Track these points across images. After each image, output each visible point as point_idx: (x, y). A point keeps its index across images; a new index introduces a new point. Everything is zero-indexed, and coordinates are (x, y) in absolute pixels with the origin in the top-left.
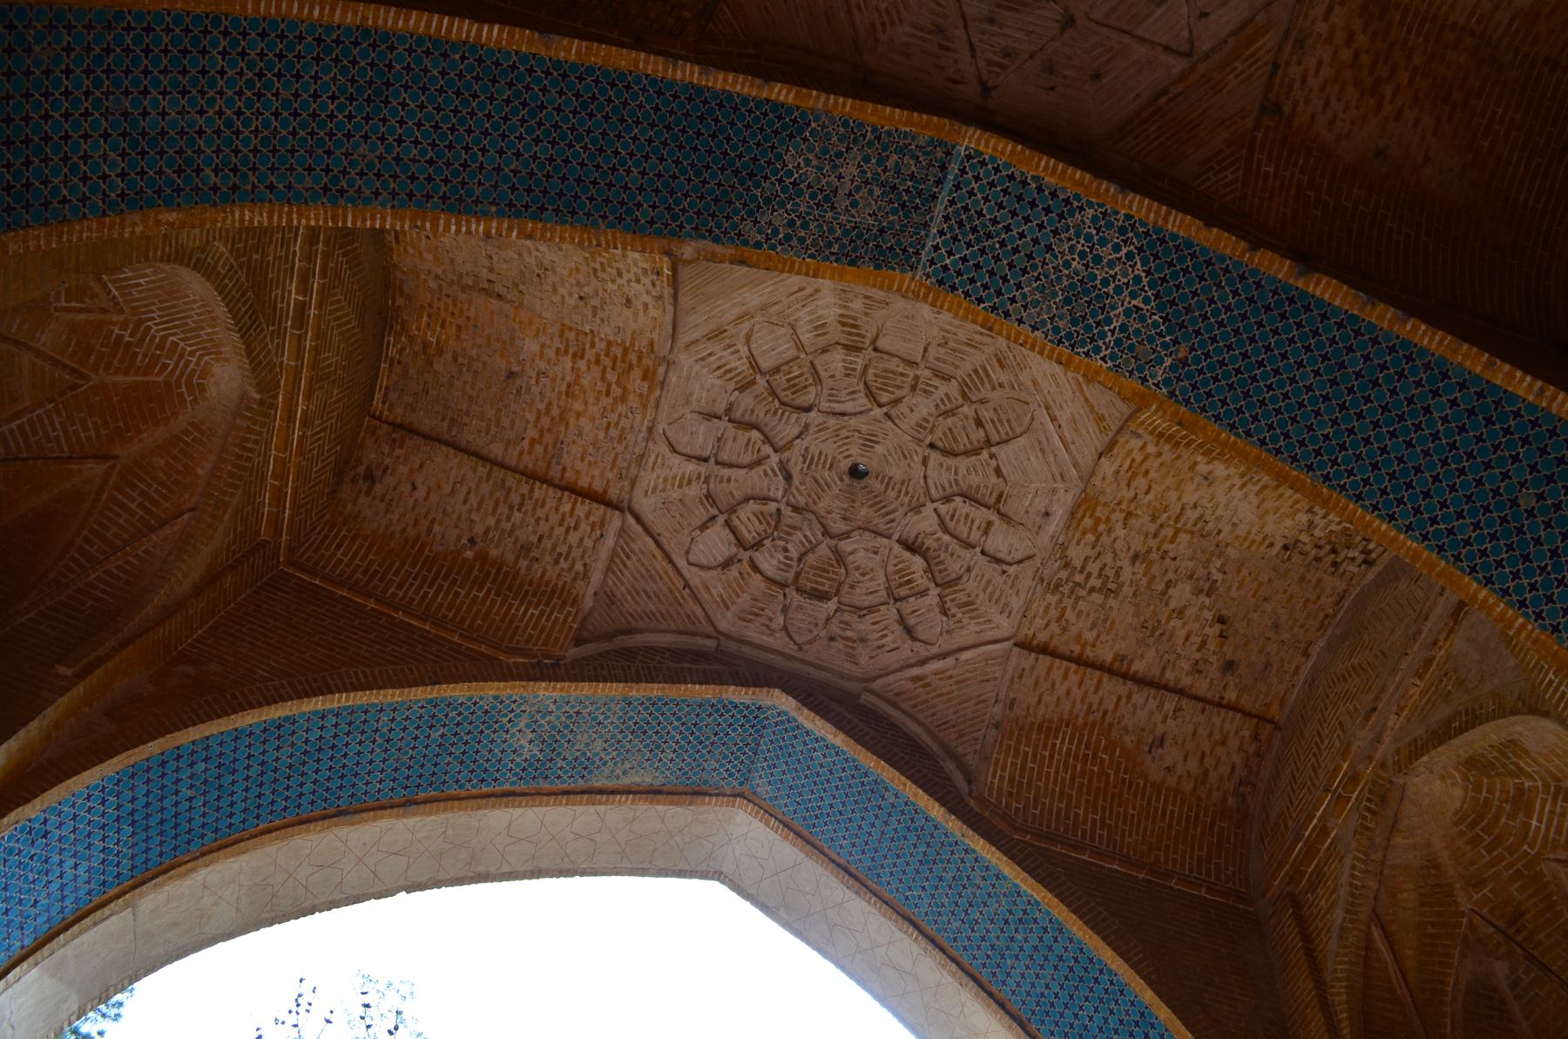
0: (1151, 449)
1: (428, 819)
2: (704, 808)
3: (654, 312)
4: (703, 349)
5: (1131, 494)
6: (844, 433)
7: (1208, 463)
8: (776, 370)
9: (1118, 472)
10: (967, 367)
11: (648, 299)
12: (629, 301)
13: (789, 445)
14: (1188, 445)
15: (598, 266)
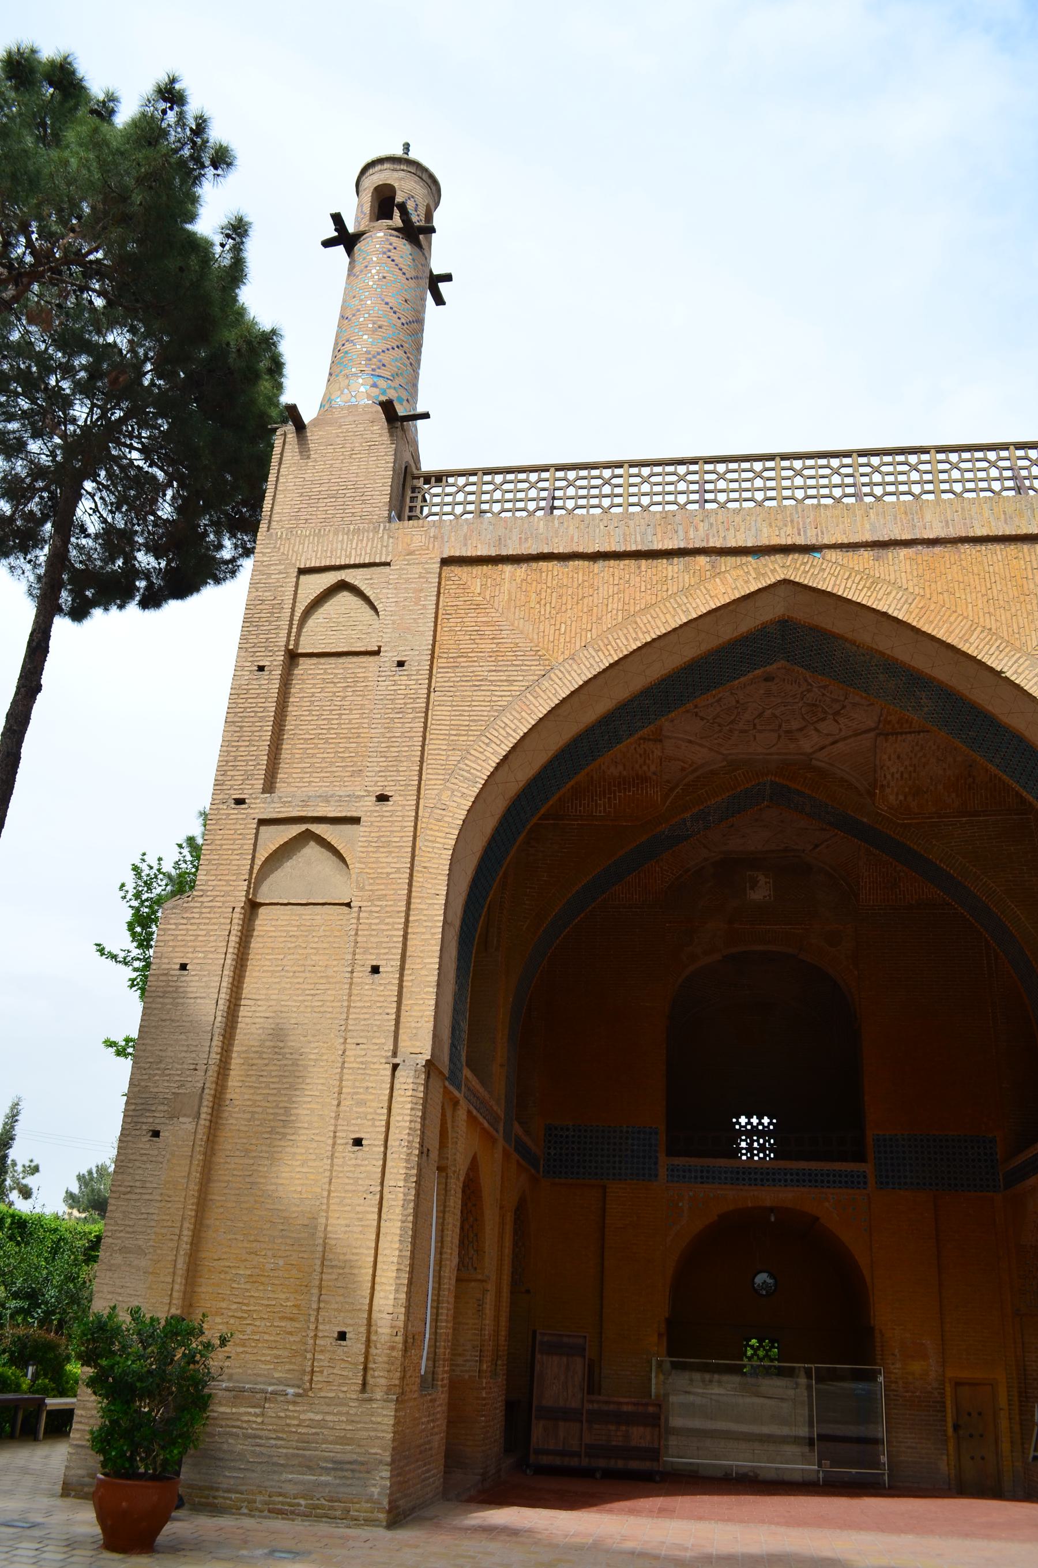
0: (645, 768)
2: (807, 620)
3: (885, 757)
5: (642, 746)
6: (783, 694)
7: (620, 773)
8: (823, 719)
9: (653, 752)
12: (899, 757)
13: (809, 691)
14: (634, 781)
15: (914, 775)
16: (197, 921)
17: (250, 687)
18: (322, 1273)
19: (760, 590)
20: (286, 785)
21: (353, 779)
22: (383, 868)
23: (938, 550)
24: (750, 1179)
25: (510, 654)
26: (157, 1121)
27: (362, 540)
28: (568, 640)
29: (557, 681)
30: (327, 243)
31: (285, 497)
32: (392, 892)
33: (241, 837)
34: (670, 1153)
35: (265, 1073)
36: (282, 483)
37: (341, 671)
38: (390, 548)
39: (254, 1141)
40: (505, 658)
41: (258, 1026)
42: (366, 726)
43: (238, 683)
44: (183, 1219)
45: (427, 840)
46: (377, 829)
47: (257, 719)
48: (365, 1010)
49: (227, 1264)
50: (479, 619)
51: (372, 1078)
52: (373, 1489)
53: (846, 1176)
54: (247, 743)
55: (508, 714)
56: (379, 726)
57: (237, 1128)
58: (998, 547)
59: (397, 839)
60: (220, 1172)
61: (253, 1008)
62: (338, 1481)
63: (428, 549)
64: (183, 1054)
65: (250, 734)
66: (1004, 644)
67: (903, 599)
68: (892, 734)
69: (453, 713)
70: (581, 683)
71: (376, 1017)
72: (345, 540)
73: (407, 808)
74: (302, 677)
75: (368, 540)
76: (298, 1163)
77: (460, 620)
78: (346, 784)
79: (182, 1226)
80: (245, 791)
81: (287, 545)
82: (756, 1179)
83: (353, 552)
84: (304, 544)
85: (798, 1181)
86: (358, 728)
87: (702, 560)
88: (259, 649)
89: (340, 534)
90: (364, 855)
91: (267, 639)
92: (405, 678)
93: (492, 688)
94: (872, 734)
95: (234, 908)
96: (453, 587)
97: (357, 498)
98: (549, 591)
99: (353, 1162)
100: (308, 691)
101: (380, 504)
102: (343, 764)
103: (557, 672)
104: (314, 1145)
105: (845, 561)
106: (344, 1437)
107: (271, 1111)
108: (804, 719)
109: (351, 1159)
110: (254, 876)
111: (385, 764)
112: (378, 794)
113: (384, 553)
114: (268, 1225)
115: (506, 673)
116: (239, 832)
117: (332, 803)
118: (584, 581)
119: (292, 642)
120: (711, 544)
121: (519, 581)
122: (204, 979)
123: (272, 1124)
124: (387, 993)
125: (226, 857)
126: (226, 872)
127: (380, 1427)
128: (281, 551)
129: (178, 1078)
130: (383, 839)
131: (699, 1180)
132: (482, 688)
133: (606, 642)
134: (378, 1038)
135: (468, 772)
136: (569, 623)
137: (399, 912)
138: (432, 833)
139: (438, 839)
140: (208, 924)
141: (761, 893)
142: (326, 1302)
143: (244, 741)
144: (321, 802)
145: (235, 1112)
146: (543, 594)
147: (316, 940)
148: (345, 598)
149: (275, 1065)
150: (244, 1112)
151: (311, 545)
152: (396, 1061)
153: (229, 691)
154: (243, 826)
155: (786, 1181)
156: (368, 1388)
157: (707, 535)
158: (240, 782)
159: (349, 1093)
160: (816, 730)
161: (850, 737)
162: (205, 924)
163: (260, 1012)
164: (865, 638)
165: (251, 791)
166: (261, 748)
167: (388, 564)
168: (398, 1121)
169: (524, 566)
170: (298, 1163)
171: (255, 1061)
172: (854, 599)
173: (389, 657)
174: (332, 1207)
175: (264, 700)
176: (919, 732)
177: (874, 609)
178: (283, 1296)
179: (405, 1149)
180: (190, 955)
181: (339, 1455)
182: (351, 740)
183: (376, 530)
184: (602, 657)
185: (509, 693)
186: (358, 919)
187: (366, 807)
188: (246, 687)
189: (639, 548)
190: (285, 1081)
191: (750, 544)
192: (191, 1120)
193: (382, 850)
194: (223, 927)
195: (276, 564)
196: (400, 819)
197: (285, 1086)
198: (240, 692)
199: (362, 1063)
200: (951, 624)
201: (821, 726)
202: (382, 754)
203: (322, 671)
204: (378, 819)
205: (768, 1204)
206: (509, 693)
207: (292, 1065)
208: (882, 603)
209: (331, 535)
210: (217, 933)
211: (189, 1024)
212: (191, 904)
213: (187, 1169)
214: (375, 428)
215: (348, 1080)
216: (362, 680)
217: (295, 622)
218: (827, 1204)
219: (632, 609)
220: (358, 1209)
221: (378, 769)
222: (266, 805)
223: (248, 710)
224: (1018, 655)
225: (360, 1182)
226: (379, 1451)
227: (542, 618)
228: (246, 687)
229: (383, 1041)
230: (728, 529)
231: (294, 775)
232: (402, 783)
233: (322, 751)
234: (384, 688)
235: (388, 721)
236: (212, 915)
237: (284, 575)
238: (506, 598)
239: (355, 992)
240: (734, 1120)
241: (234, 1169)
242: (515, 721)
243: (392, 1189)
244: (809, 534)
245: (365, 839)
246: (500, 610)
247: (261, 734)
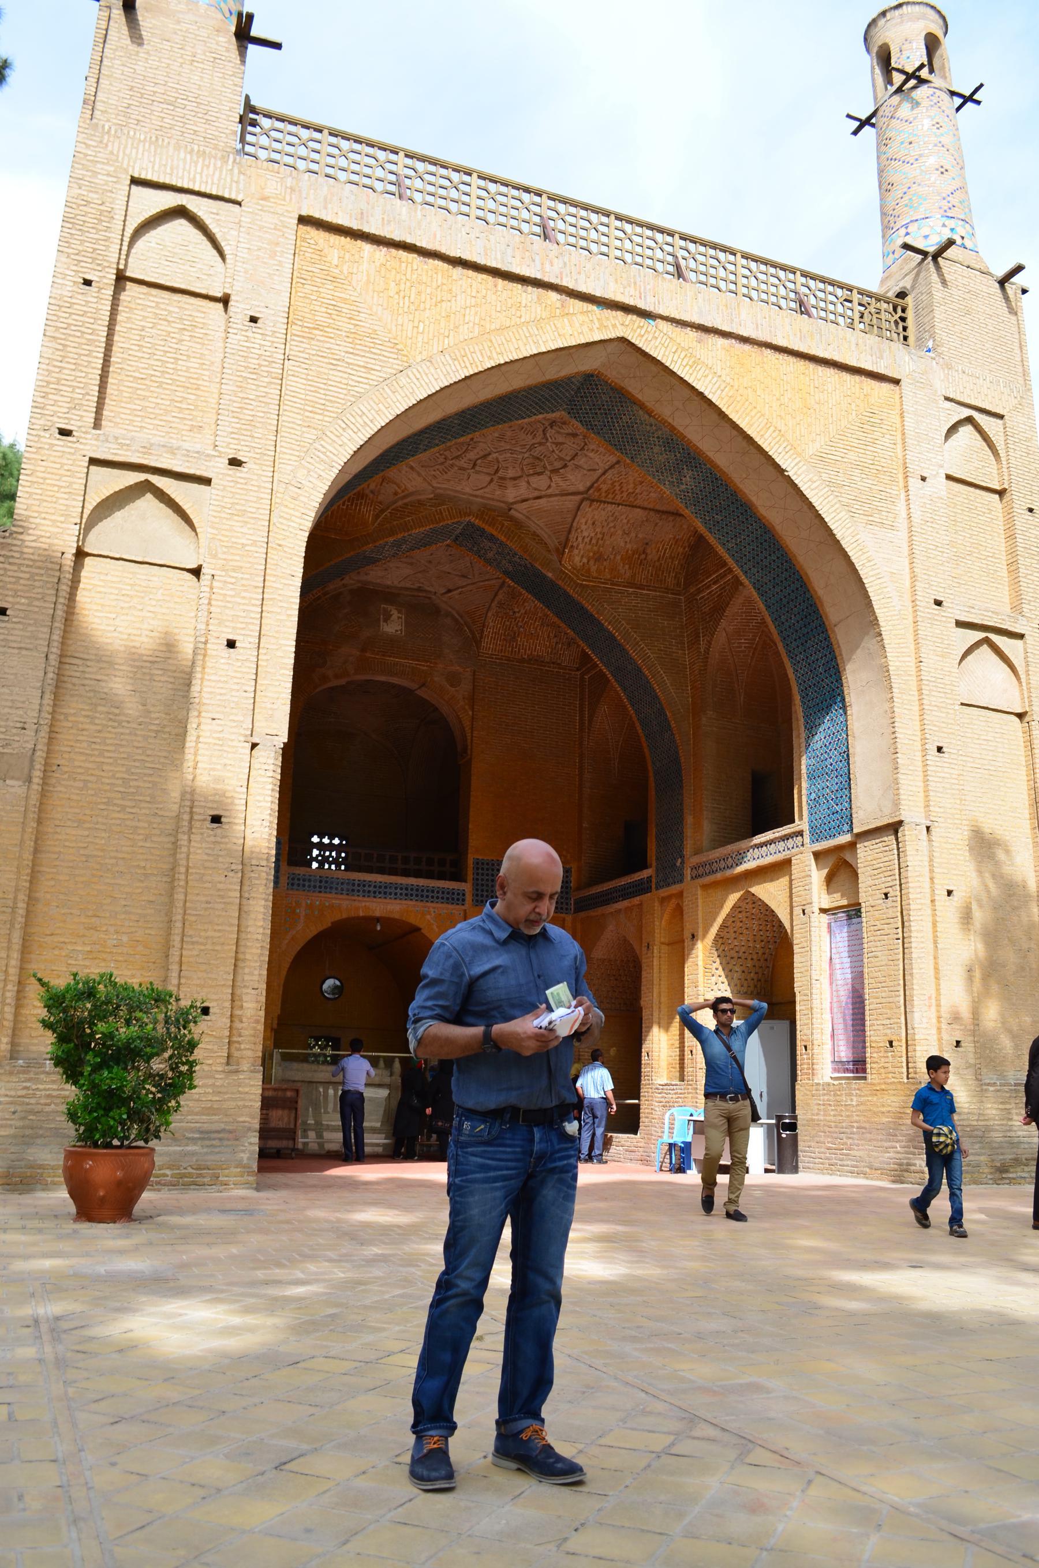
1: (747, 491)
3: (583, 521)
4: (572, 489)
6: (513, 442)
8: (539, 474)
10: (449, 473)
11: (584, 527)
12: (593, 523)
13: (540, 444)
15: (600, 542)
16: (17, 561)
17: (74, 301)
18: (182, 949)
19: (601, 341)
20: (112, 424)
21: (191, 434)
22: (237, 537)
23: (747, 347)
24: (364, 891)
25: (368, 339)
27: (208, 166)
28: (426, 340)
29: (415, 380)
31: (111, 84)
32: (248, 565)
33: (69, 473)
35: (98, 740)
36: (108, 67)
37: (177, 310)
38: (241, 186)
39: (88, 812)
40: (362, 342)
41: (87, 688)
42: (206, 378)
43: (59, 292)
44: (17, 890)
45: (281, 517)
46: (231, 495)
47: (84, 341)
48: (221, 685)
49: (62, 940)
50: (336, 294)
51: (230, 755)
52: (242, 1155)
53: (448, 893)
54: (73, 367)
55: (365, 403)
56: (231, 383)
57: (67, 796)
58: (791, 359)
59: (254, 510)
60: (49, 843)
61: (81, 668)
62: (205, 1150)
63: (284, 200)
64: (7, 710)
65: (76, 356)
66: (789, 447)
67: (717, 385)
68: (597, 501)
69: (309, 388)
70: (438, 389)
71: (234, 693)
72: (188, 160)
73: (264, 479)
74: (130, 305)
75: (215, 169)
76: (141, 837)
77: (316, 289)
78: (184, 438)
79: (15, 898)
80: (72, 422)
81: (116, 144)
82: (369, 892)
83: (198, 177)
84: (137, 148)
85: (406, 895)
86: (197, 379)
87: (553, 296)
88: (85, 259)
89: (182, 151)
90: (217, 520)
91: (95, 249)
92: (260, 337)
93: (349, 371)
94: (578, 498)
95: (63, 553)
96: (309, 250)
97: (200, 115)
98: (408, 283)
99: (212, 839)
100: (137, 322)
101: (227, 131)
102: (181, 415)
103: (414, 371)
104: (158, 820)
105: (674, 336)
106: (211, 1108)
107: (107, 781)
108: (522, 469)
109: (209, 836)
110: (84, 521)
111: (238, 426)
112: (231, 457)
113: (234, 189)
114: (109, 900)
115: (364, 359)
116: (66, 467)
117: (178, 457)
118: (443, 284)
119: (122, 262)
120: (564, 284)
121: (378, 264)
122: (30, 629)
123: (109, 795)
124: (245, 670)
125: (51, 493)
126: (53, 511)
127: (247, 1097)
128: (110, 148)
130: (238, 507)
131: (318, 889)
132: (339, 368)
133: (463, 353)
134: (236, 715)
135: (324, 453)
136: (427, 323)
137: (256, 587)
138: (286, 510)
139: (293, 518)
140: (31, 566)
141: (393, 626)
142: (187, 978)
143: (68, 362)
144: (167, 452)
145: (64, 779)
146: (402, 287)
147: (154, 603)
148: (181, 225)
149: (109, 732)
150: (75, 779)
151: (146, 153)
152: (255, 740)
154: (70, 462)
155: (396, 894)
156: (232, 1061)
157: (561, 273)
158: (66, 410)
159: (205, 769)
160: (528, 483)
161: (556, 495)
162: (28, 566)
163: (89, 673)
164: (665, 411)
165: (79, 424)
166: (90, 376)
167: (239, 204)
168: (259, 801)
169: (384, 250)
170: (141, 837)
171: (87, 727)
172: (679, 373)
174: (190, 883)
175: (92, 321)
176: (619, 505)
177: (693, 387)
178: (129, 973)
179: (267, 829)
180: (10, 599)
181: (205, 1125)
182: (189, 391)
183: (224, 160)
184: (458, 367)
185: (366, 381)
186: (212, 588)
187: (215, 468)
188: (69, 300)
189: (499, 266)
190: (121, 750)
191: (598, 294)
192: (20, 783)
193: (236, 518)
194: (52, 573)
195: (103, 163)
196: (256, 489)
197: (123, 756)
198: (62, 304)
199: (219, 739)
200: (752, 417)
201: (533, 479)
202: (235, 415)
203: (153, 304)
204: (232, 484)
205: (378, 914)
206: (366, 381)
207: (130, 734)
208: (700, 383)
209: (171, 148)
210: (44, 578)
211: (12, 677)
212: (9, 541)
213: (19, 836)
214: (221, 39)
215: (204, 755)
216: (201, 326)
217: (127, 240)
218: (428, 917)
219: (488, 327)
220: (220, 886)
221: (231, 430)
222: (100, 443)
223: (73, 328)
224: (798, 459)
225: (220, 859)
226: (247, 1119)
227: (401, 311)
228: (69, 300)
229: (242, 718)
230: (579, 273)
231: (122, 416)
232: (257, 450)
233: (155, 395)
234: (236, 342)
235: (240, 379)
237: (115, 180)
238: (365, 278)
239: (208, 664)
241: (66, 840)
242: (372, 411)
243: (254, 868)
244: (648, 300)
245: (217, 503)
246: (358, 289)
247: (90, 359)
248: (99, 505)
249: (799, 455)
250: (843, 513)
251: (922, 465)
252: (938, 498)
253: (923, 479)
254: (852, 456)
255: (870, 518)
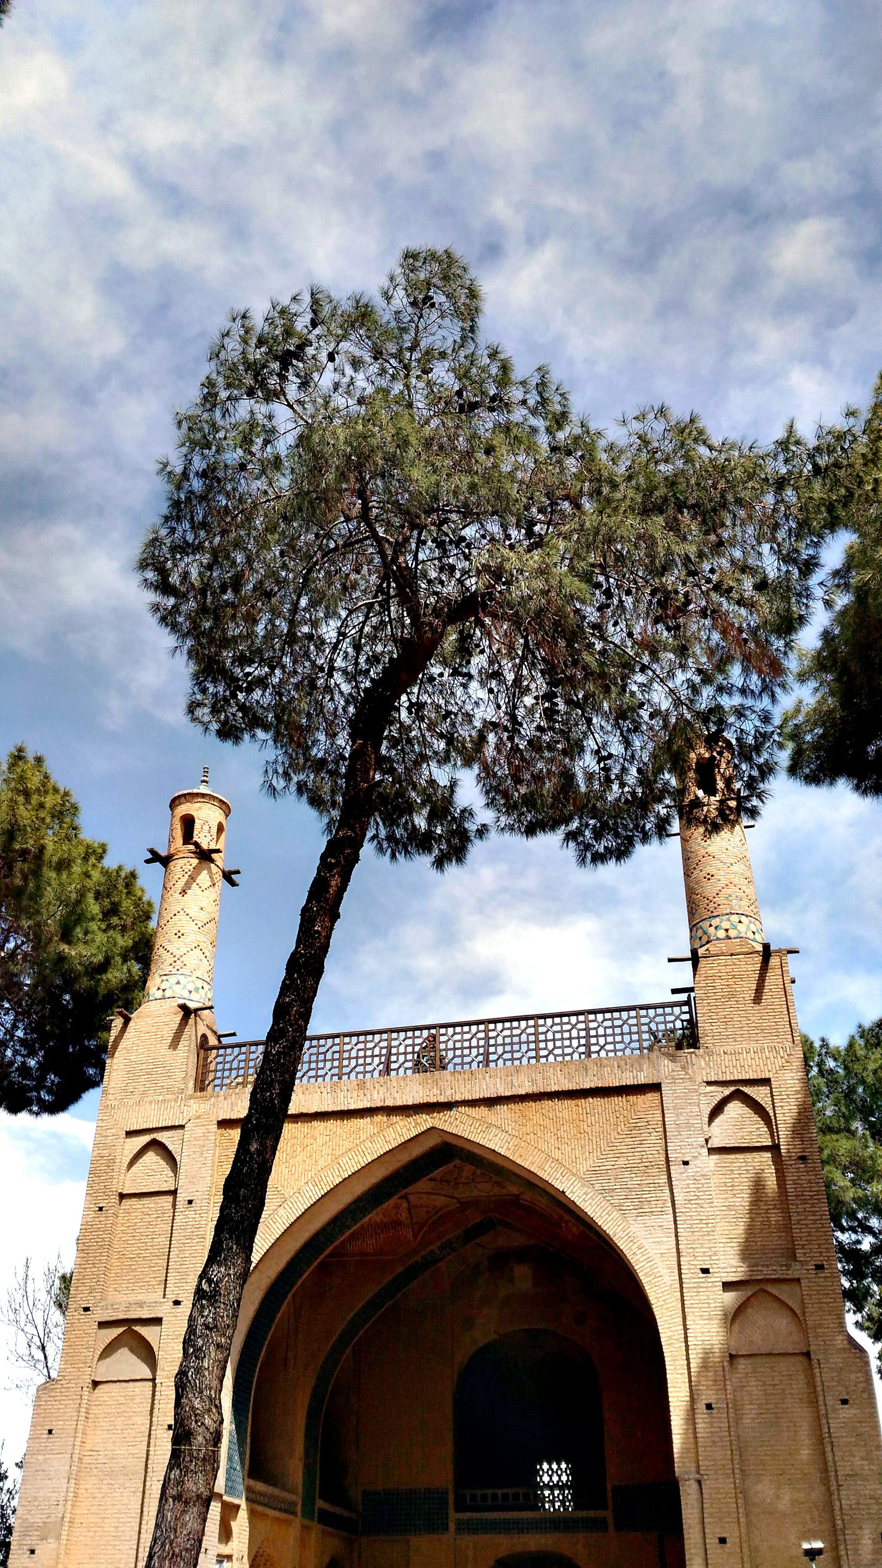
26: (34, 1542)
30: (148, 861)
34: (458, 1509)
129: (46, 1512)
153: (79, 1227)
173: (182, 1197)
236: (68, 1394)
240: (538, 1467)
248: (104, 1350)
249: (574, 1175)
250: (615, 1213)
251: (683, 1151)
252: (702, 1175)
253: (686, 1163)
254: (622, 1162)
255: (641, 1211)
